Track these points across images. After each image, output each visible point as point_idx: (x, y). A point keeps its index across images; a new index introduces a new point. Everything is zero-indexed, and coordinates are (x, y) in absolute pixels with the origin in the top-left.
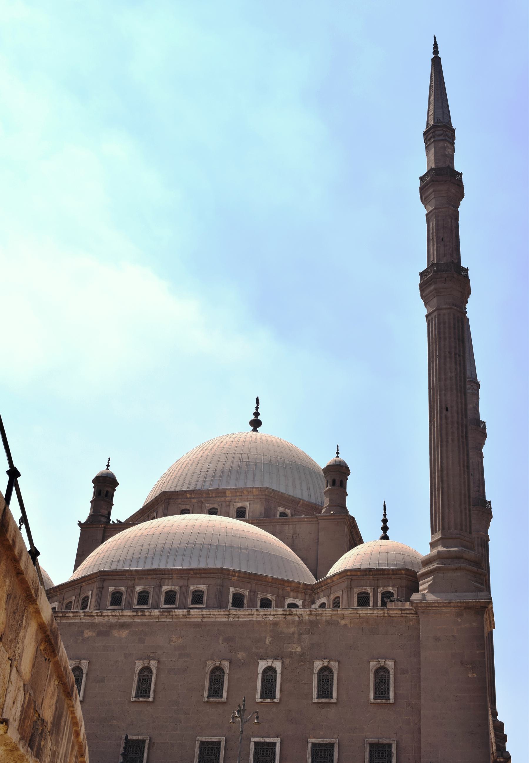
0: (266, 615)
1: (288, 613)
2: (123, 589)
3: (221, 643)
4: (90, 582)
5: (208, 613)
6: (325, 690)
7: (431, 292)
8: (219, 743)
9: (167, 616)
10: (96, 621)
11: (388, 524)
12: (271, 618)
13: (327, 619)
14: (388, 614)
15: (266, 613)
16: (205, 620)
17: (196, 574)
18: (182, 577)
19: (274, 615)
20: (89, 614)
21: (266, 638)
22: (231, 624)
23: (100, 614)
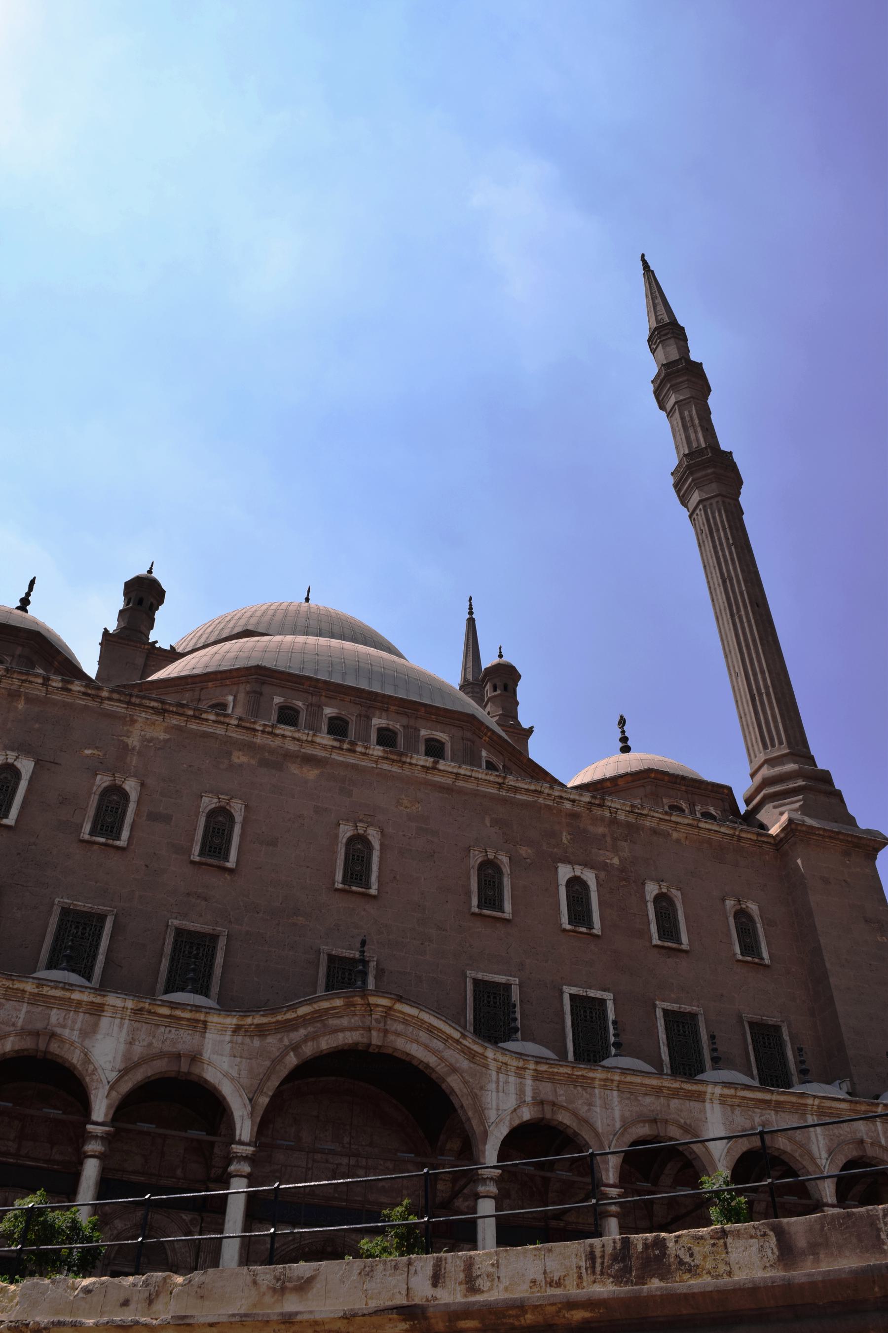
0: (561, 797)
1: (597, 802)
2: (300, 704)
3: (488, 825)
4: (228, 682)
5: (469, 773)
6: (668, 929)
7: (706, 476)
8: (507, 987)
9: (393, 761)
10: (259, 740)
11: (629, 743)
12: (568, 805)
14: (739, 836)
15: (564, 795)
16: (460, 783)
18: (405, 714)
19: (574, 801)
20: (248, 725)
21: (561, 833)
22: (504, 801)
23: (270, 729)
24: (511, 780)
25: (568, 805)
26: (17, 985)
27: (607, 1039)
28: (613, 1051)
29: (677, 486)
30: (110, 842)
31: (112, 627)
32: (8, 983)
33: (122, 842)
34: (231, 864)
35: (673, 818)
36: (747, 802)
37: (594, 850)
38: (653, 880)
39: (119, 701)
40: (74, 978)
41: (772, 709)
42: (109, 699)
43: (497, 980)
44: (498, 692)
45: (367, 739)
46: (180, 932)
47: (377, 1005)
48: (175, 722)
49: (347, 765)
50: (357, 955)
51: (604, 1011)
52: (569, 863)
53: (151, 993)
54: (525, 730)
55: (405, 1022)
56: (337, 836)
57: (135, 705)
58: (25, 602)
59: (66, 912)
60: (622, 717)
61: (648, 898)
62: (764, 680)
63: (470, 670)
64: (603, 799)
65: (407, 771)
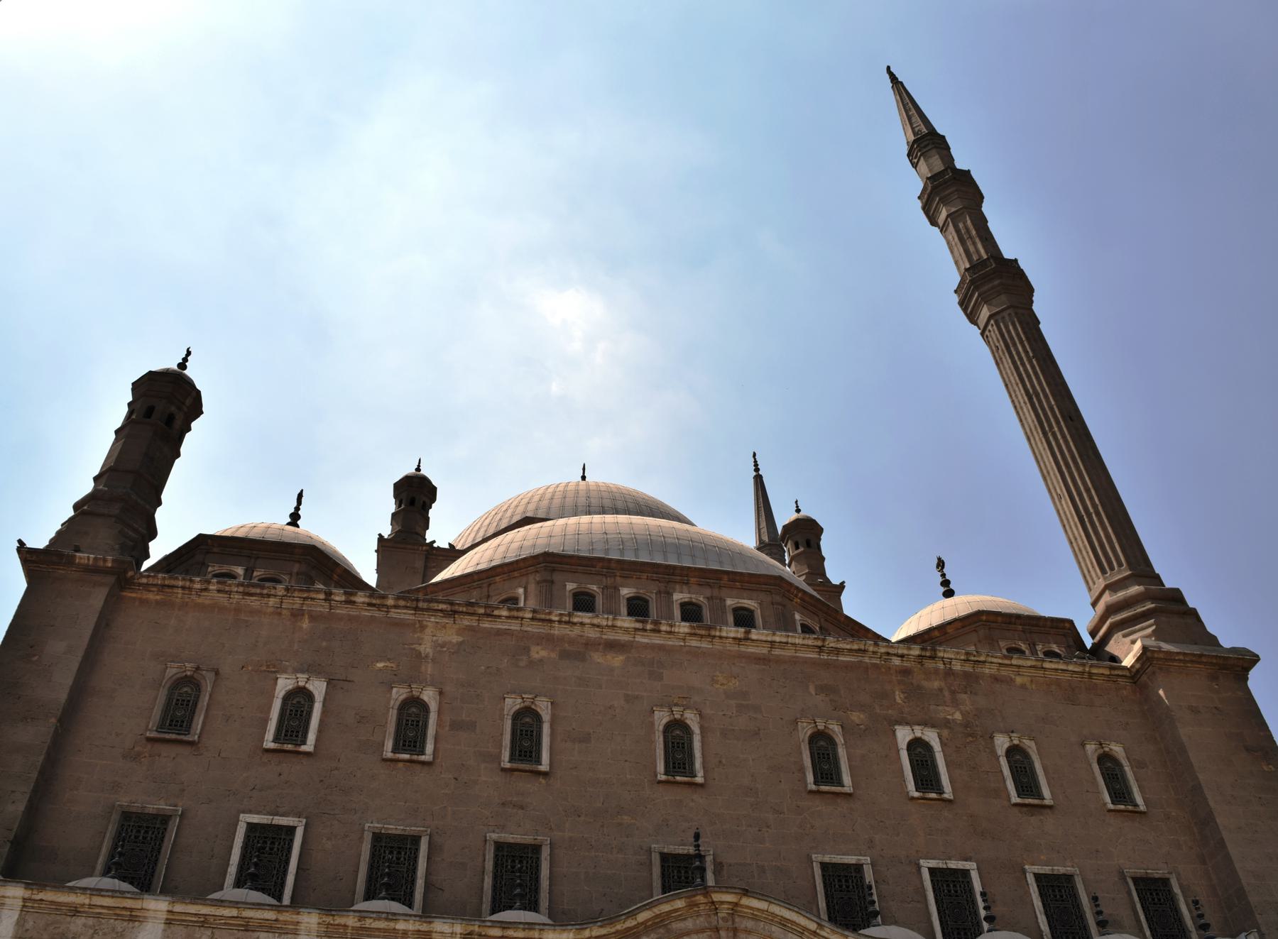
0: (888, 654)
1: (928, 654)
2: (595, 588)
4: (516, 574)
5: (784, 640)
6: (1027, 785)
7: (993, 288)
8: (858, 868)
9: (702, 636)
10: (557, 630)
11: (952, 586)
13: (993, 672)
15: (891, 651)
16: (777, 652)
17: (734, 581)
19: (902, 656)
20: (543, 616)
22: (827, 665)
24: (831, 642)
25: (896, 661)
26: (339, 920)
27: (976, 913)
28: (986, 926)
29: (963, 304)
30: (415, 757)
31: (387, 531)
32: (329, 919)
33: (427, 757)
34: (544, 767)
35: (1014, 662)
36: (1093, 634)
37: (932, 707)
38: (1001, 732)
39: (406, 607)
40: (395, 907)
41: (1105, 529)
42: (396, 607)
43: (846, 861)
44: (801, 549)
45: (670, 616)
46: (499, 846)
47: (722, 903)
48: (466, 623)
49: (652, 647)
50: (692, 850)
51: (970, 883)
52: (907, 724)
53: (477, 915)
54: (835, 586)
55: (755, 918)
56: (652, 724)
57: (422, 610)
58: (295, 518)
59: (377, 837)
60: (939, 559)
61: (999, 753)
62: (1091, 499)
63: (764, 530)
64: (935, 650)
65: (718, 646)
